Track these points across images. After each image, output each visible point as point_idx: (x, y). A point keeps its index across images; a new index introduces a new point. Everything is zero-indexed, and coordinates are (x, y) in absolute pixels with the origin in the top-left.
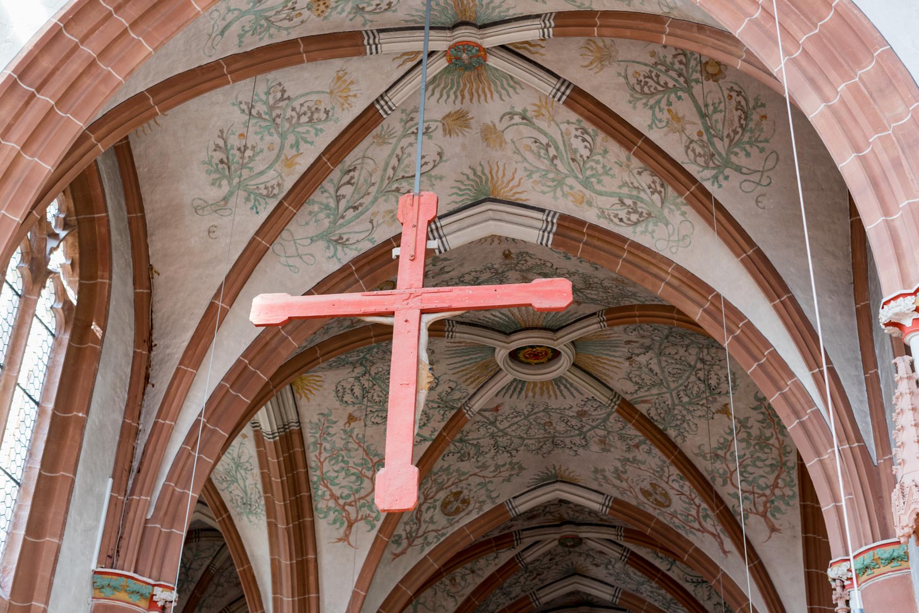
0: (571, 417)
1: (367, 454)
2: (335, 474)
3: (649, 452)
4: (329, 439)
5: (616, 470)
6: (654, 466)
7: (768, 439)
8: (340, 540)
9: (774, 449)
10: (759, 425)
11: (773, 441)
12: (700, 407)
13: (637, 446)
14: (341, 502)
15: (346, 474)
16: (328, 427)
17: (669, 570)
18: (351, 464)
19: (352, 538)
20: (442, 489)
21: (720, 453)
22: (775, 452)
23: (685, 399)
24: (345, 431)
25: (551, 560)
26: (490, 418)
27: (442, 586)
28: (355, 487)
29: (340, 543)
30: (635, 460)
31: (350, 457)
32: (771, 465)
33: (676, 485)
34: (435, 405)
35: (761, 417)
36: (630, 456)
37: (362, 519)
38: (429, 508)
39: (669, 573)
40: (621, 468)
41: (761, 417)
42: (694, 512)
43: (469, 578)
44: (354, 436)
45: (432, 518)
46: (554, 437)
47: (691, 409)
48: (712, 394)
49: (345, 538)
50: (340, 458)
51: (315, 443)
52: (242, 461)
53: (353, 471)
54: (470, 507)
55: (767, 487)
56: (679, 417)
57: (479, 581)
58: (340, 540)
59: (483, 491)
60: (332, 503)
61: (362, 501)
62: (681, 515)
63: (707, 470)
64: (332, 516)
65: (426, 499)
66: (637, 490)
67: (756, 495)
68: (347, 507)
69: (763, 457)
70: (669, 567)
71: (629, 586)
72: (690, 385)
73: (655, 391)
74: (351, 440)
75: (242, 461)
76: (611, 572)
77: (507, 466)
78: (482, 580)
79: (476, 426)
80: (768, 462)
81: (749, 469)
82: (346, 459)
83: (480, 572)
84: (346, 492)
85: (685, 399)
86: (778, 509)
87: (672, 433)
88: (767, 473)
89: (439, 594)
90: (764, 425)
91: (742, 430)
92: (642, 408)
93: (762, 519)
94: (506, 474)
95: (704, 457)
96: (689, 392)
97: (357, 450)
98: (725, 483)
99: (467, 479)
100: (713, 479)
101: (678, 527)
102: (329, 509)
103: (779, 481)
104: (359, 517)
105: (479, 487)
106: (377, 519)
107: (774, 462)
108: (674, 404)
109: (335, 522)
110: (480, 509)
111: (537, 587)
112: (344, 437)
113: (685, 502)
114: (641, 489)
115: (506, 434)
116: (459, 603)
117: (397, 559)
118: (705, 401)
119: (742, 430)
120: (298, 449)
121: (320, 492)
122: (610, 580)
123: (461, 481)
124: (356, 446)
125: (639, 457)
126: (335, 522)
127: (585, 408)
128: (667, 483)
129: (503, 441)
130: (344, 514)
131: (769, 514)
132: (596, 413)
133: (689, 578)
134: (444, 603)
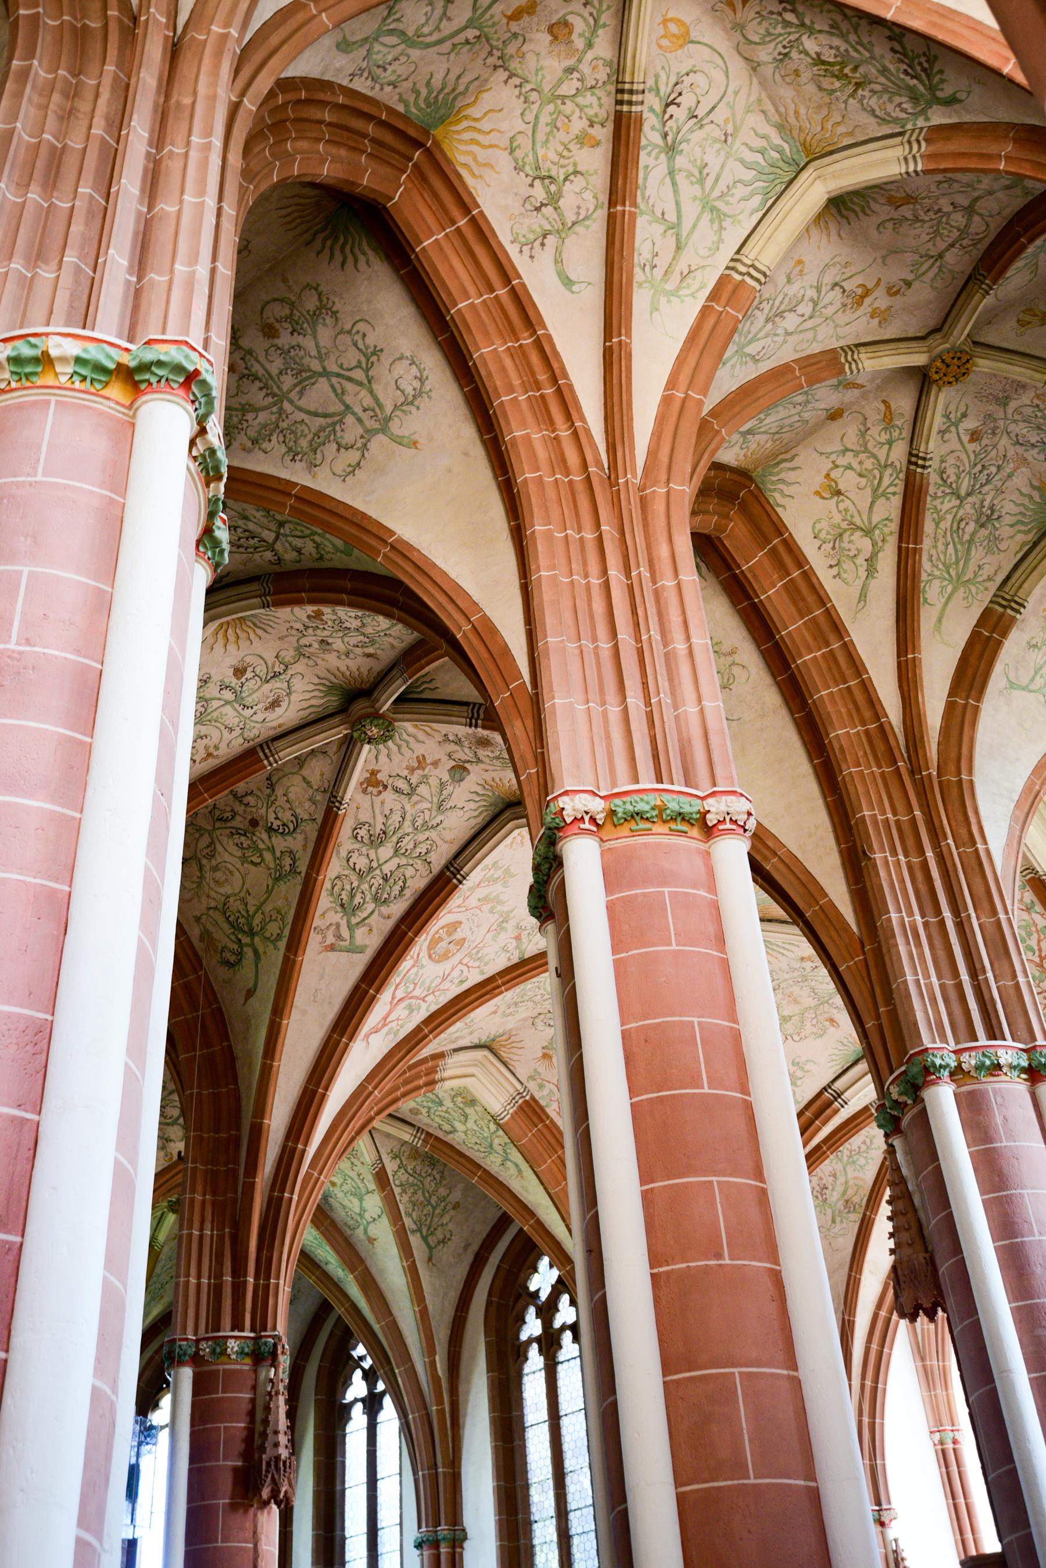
3: (505, 949)
5: (501, 903)
6: (485, 951)
30: (501, 928)
33: (456, 973)
36: (510, 926)
40: (499, 908)
42: (417, 992)
62: (416, 974)
113: (432, 982)
114: (460, 923)
125: (503, 935)
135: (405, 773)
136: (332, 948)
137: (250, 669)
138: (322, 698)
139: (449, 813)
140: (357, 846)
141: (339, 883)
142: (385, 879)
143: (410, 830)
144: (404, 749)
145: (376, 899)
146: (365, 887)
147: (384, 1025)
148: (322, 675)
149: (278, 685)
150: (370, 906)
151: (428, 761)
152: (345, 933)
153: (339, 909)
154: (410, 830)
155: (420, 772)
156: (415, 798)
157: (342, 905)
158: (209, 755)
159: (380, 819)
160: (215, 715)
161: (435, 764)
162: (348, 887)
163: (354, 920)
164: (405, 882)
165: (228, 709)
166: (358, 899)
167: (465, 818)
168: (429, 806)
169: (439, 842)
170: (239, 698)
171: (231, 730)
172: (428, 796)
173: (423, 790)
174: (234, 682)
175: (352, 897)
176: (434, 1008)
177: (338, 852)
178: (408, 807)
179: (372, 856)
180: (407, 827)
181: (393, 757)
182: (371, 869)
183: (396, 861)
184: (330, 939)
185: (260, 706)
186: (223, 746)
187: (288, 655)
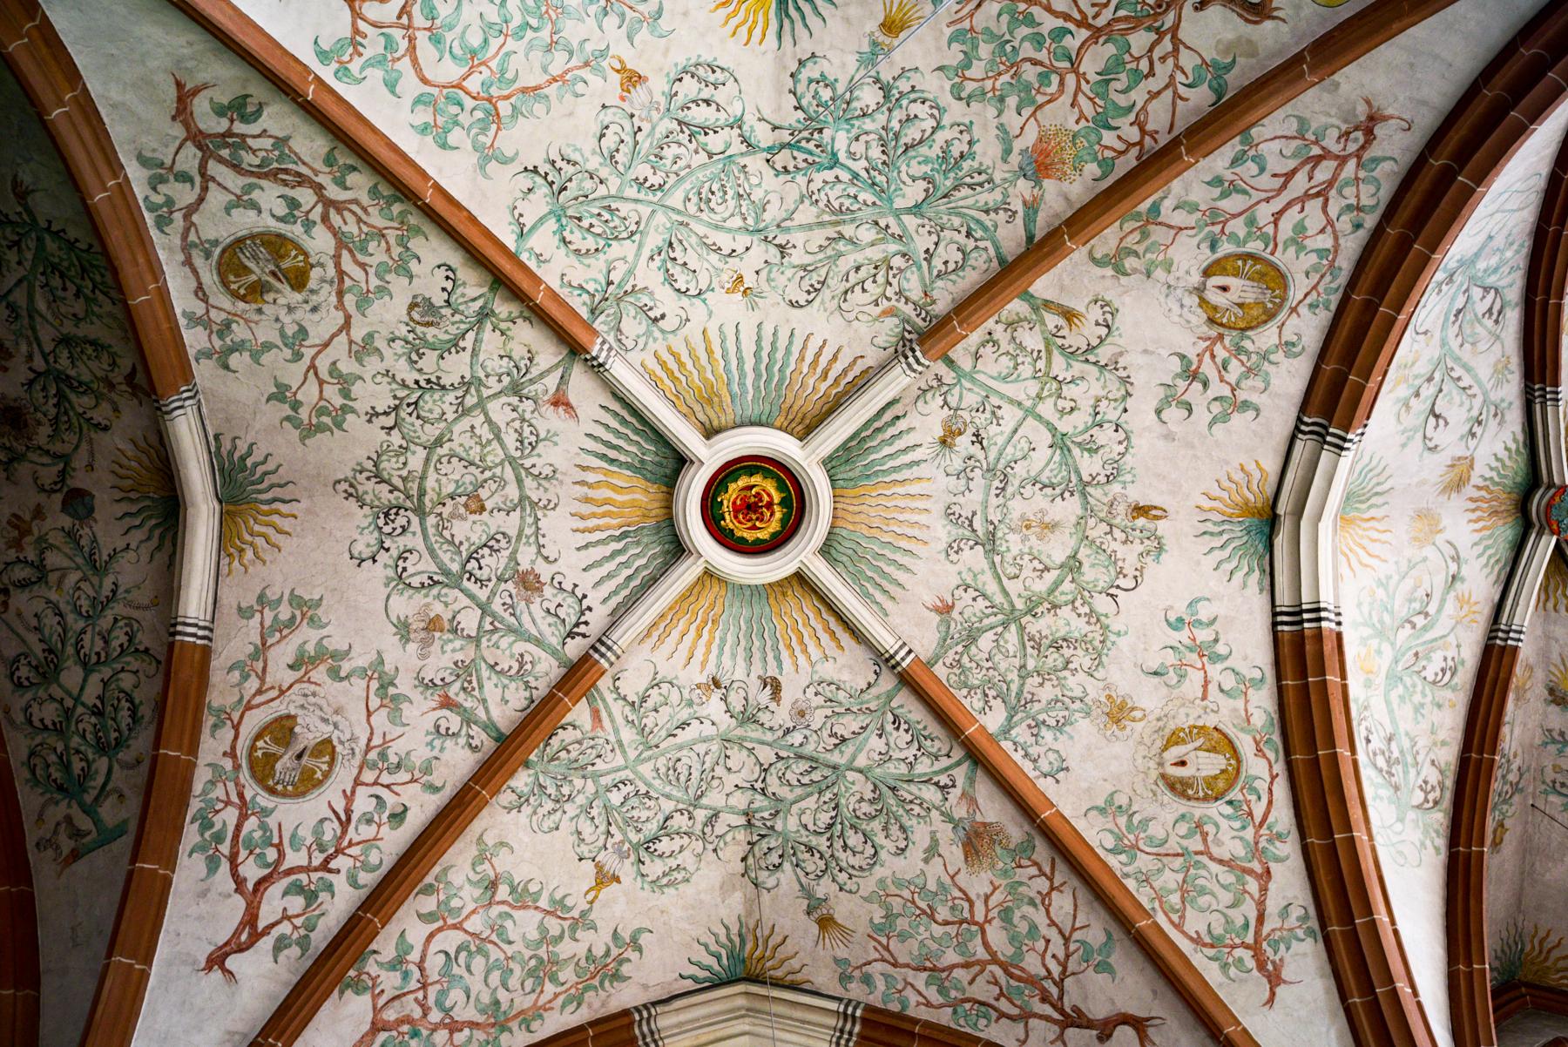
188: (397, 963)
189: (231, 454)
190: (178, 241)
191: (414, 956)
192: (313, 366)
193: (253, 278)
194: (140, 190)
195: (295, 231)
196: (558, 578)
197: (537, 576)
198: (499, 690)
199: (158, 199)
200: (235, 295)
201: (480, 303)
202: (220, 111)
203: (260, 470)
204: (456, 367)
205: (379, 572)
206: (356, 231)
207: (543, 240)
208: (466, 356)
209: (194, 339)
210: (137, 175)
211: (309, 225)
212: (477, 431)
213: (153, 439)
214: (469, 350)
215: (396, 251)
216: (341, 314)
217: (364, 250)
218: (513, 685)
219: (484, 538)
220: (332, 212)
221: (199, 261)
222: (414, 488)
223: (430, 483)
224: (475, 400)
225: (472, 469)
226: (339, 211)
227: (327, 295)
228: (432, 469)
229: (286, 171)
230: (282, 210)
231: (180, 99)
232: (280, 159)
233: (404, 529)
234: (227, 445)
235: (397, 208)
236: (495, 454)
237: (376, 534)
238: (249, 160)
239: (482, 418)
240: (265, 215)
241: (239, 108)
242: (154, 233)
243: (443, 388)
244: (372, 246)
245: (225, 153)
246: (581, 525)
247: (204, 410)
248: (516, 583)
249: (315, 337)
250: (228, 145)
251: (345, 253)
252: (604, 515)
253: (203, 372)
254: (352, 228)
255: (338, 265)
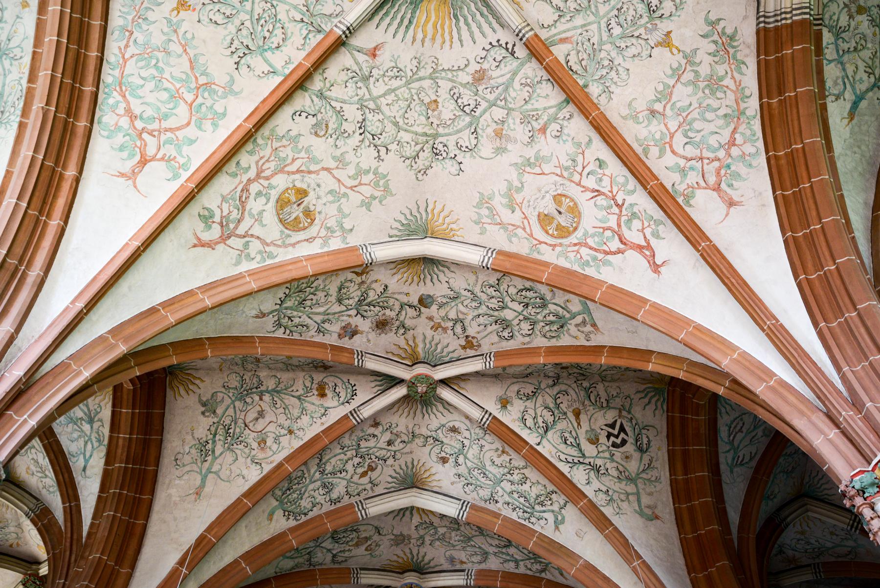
0: (465, 86)
1: (192, 68)
2: (142, 82)
4: (145, 27)
7: (721, 79)
8: (122, 175)
9: (729, 92)
10: (710, 59)
11: (728, 82)
12: (634, 40)
13: (543, 130)
14: (139, 125)
15: (156, 87)
16: (147, 9)
17: (539, 444)
18: (166, 75)
19: (140, 179)
20: (282, 171)
21: (658, 107)
22: (731, 96)
23: (617, 31)
24: (169, 21)
25: (390, 443)
26: (364, 66)
27: (247, 450)
28: (164, 110)
29: (122, 180)
31: (168, 64)
32: (725, 115)
33: (590, 182)
34: (298, 17)
35: (712, 48)
36: (530, 153)
37: (162, 159)
38: (259, 194)
39: (538, 448)
41: (712, 48)
42: (612, 222)
43: (284, 440)
44: (181, 32)
45: (261, 213)
46: (435, 136)
47: (623, 45)
48: (651, 18)
49: (132, 176)
50: (154, 62)
51: (124, 29)
52: (11, 46)
53: (166, 84)
54: (313, 231)
55: (721, 146)
56: (606, 63)
57: (297, 444)
58: (122, 175)
59: (332, 210)
60: (124, 122)
61: (169, 134)
62: (593, 236)
63: (637, 140)
64: (119, 139)
65: (258, 176)
66: (534, 220)
67: (706, 161)
68: (145, 136)
69: (715, 104)
70: (538, 440)
71: (482, 493)
72: (625, 7)
73: (579, 21)
74: (174, 38)
75: (11, 46)
76: (462, 469)
77: (371, 176)
78: (301, 443)
79: (344, 76)
80: (721, 112)
81: (697, 125)
82: (160, 64)
83: (300, 433)
84: (149, 112)
85: (617, 31)
86: (737, 176)
87: (594, 90)
88: (719, 128)
89: (241, 460)
90: (716, 59)
91: (689, 68)
92: (559, 52)
93: (715, 194)
94: (367, 191)
95: (635, 118)
96: (622, 18)
97: (180, 56)
98: (662, 153)
99: (317, 172)
100: (646, 151)
101: (587, 263)
102: (117, 127)
103: (737, 136)
104: (159, 156)
105: (330, 198)
106: (185, 167)
107: (729, 111)
108: (601, 42)
109: (122, 148)
110: (326, 241)
111: (363, 495)
112: (166, 30)
115: (378, 110)
116: (265, 473)
117: (200, 249)
118: (642, 31)
119: (689, 68)
120: (96, 23)
121: (111, 101)
122: (457, 490)
123: (310, 172)
124: (180, 50)
126: (122, 148)
127: (485, 66)
128: (579, 184)
129: (373, 124)
130: (138, 143)
131: (723, 186)
132: (498, 73)
133: (563, 457)
134: (245, 472)
135: (450, 332)
136: (594, 325)
137: (440, 456)
138: (436, 406)
139: (456, 289)
140: (517, 333)
141: (548, 335)
142: (526, 305)
143: (483, 307)
144: (436, 341)
145: (544, 306)
146: (540, 317)
147: (649, 247)
148: (421, 415)
149: (441, 435)
150: (552, 307)
151: (432, 323)
152: (579, 319)
153: (565, 328)
154: (483, 307)
155: (443, 324)
156: (461, 316)
157: (562, 327)
158: (503, 452)
159: (490, 329)
160: (476, 461)
161: (430, 318)
162: (547, 328)
163: (568, 316)
164: (522, 290)
165: (470, 455)
166: (551, 318)
167: (453, 275)
168: (460, 305)
169: (480, 283)
170: (460, 452)
171: (482, 446)
172: (454, 310)
173: (452, 315)
174: (452, 460)
175: (552, 323)
176: (632, 183)
177: (529, 343)
178: (470, 317)
179: (516, 322)
180: (483, 309)
181: (445, 344)
182: (526, 318)
183: (510, 304)
184: (589, 328)
185: (459, 437)
186: (494, 447)
187: (419, 441)
188: (683, 172)
189: (400, 230)
190: (281, 250)
191: (682, 162)
192: (351, 188)
193: (301, 215)
194: (253, 265)
195: (274, 194)
196: (478, 59)
197: (476, 72)
198: (540, 99)
199: (259, 257)
200: (311, 224)
201: (314, 98)
202: (208, 227)
203: (409, 217)
204: (352, 113)
205: (466, 159)
206: (274, 163)
207: (278, 60)
208: (346, 107)
209: (336, 244)
210: (245, 266)
211: (270, 187)
212: (390, 102)
213: (393, 266)
214: (342, 105)
215: (284, 142)
216: (321, 172)
217: (284, 159)
218: (538, 91)
219: (453, 102)
220: (263, 175)
221: (292, 240)
222: (422, 139)
223: (420, 130)
224: (371, 102)
225: (412, 106)
226: (263, 171)
227: (311, 179)
228: (411, 128)
229: (240, 197)
230: (263, 200)
231: (203, 246)
232: (234, 199)
233: (445, 146)
234: (396, 232)
235: (260, 141)
236: (404, 93)
237: (447, 161)
238: (235, 215)
239: (382, 99)
240: (265, 208)
241: (206, 218)
242: (277, 260)
243: (364, 120)
244: (282, 155)
245: (232, 226)
246: (448, 43)
247: (375, 242)
248: (479, 85)
249: (335, 186)
250: (227, 224)
251: (286, 169)
252: (443, 29)
253: (353, 241)
254: (272, 165)
255: (293, 173)
